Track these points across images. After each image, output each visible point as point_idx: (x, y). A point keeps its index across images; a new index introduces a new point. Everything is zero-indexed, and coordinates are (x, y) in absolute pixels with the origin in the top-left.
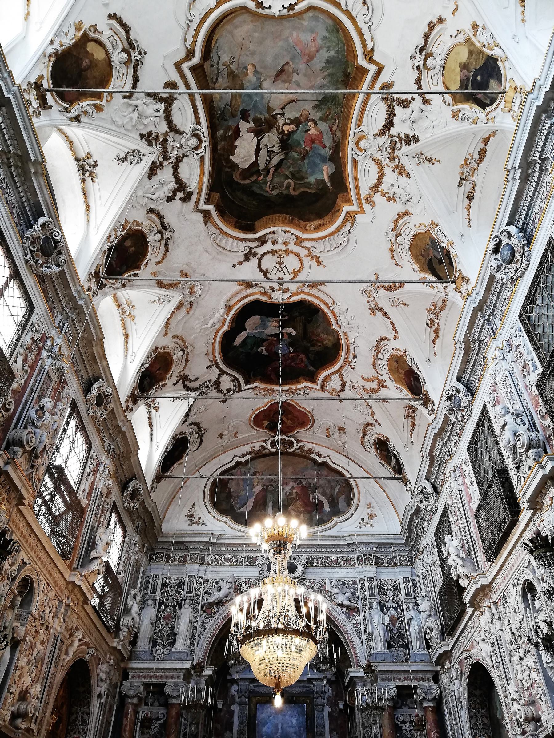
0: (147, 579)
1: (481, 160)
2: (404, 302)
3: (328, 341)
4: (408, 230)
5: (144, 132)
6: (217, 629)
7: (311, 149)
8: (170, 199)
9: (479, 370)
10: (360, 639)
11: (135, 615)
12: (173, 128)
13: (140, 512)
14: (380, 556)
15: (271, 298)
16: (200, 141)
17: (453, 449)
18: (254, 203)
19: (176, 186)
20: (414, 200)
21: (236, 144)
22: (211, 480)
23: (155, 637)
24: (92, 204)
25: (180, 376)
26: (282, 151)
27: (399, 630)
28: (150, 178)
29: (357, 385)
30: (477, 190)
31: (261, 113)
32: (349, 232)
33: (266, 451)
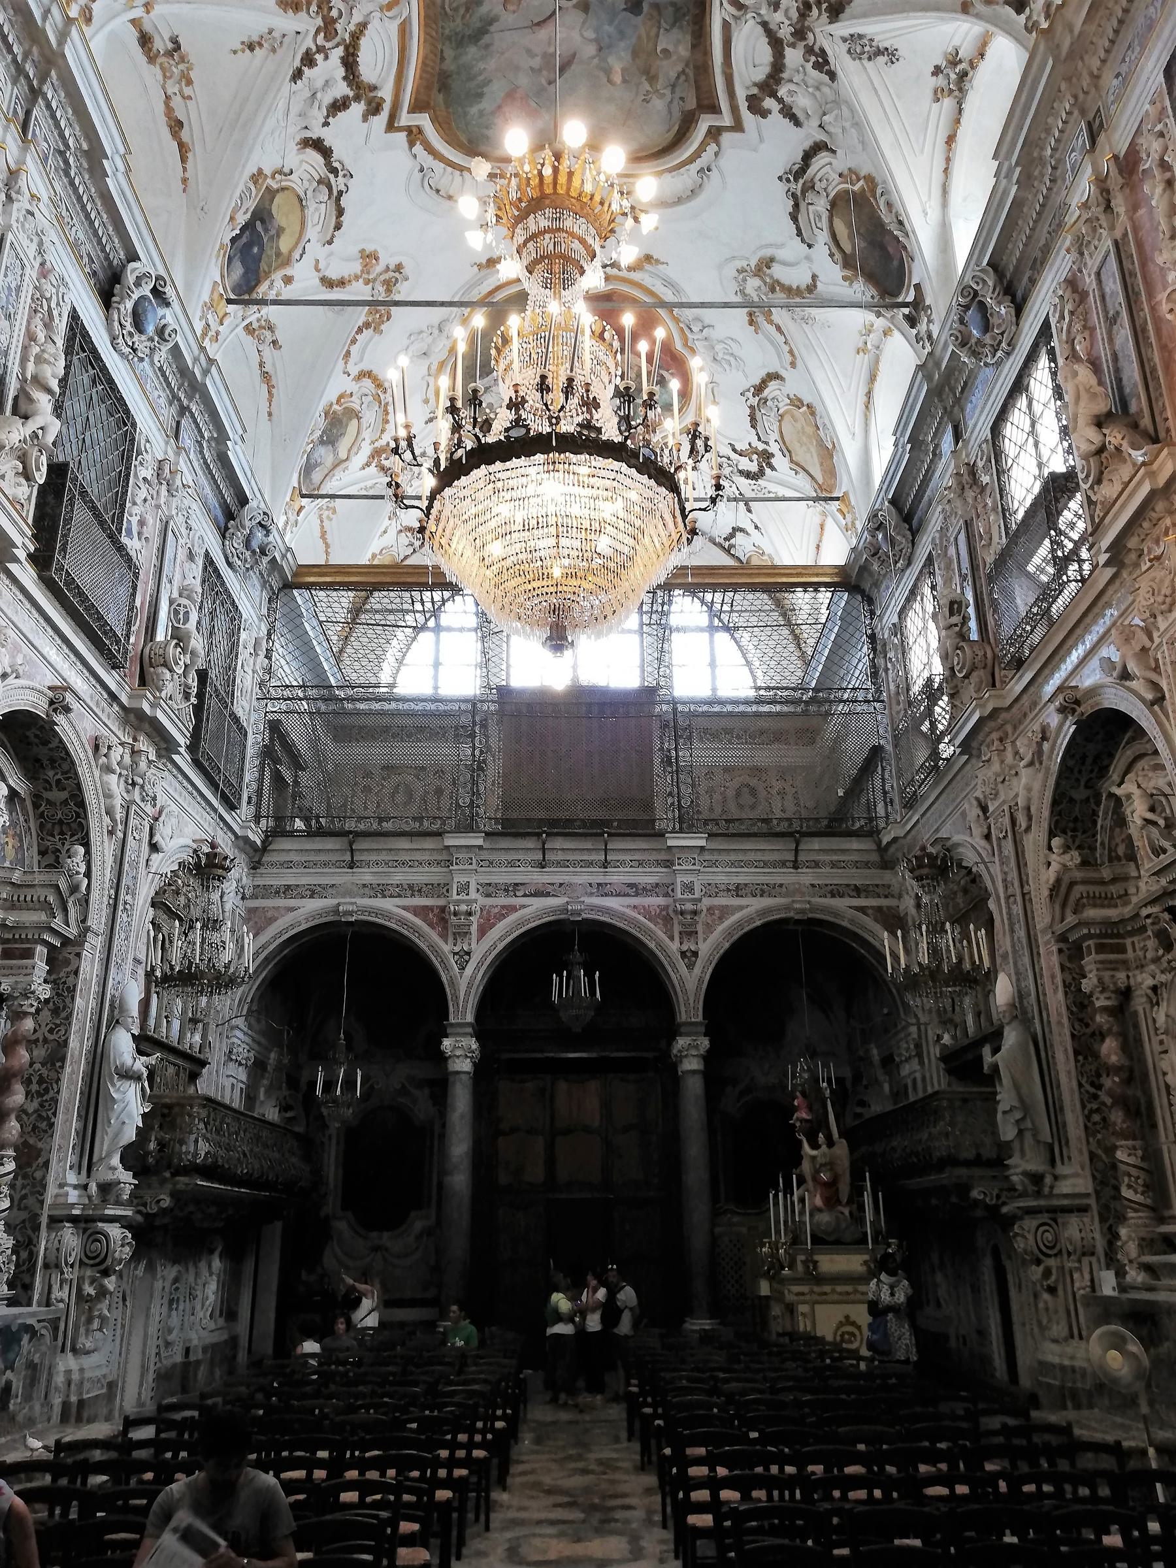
1: (169, 110)
12: (776, 44)
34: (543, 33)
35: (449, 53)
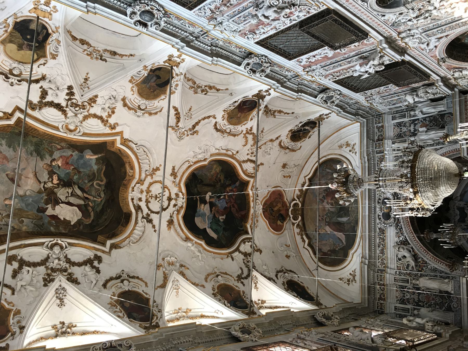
0: (398, 316)
1: (88, 44)
2: (188, 109)
3: (217, 169)
4: (136, 100)
5: (43, 283)
6: (435, 258)
7: (73, 165)
8: (98, 271)
9: (233, 49)
10: (438, 150)
11: (424, 320)
12: (44, 262)
13: (342, 317)
14: (376, 138)
15: (182, 207)
16: (56, 244)
17: (292, 73)
18: (109, 211)
19: (88, 265)
20: (114, 94)
21: (62, 219)
22: (320, 264)
23: (444, 309)
24: (92, 329)
25: (237, 280)
26: (72, 186)
27: (430, 121)
28: (79, 283)
29: (250, 151)
30: (109, 48)
31: (42, 198)
32: (136, 144)
33: (300, 224)
34: (31, 175)
35: (35, 140)
